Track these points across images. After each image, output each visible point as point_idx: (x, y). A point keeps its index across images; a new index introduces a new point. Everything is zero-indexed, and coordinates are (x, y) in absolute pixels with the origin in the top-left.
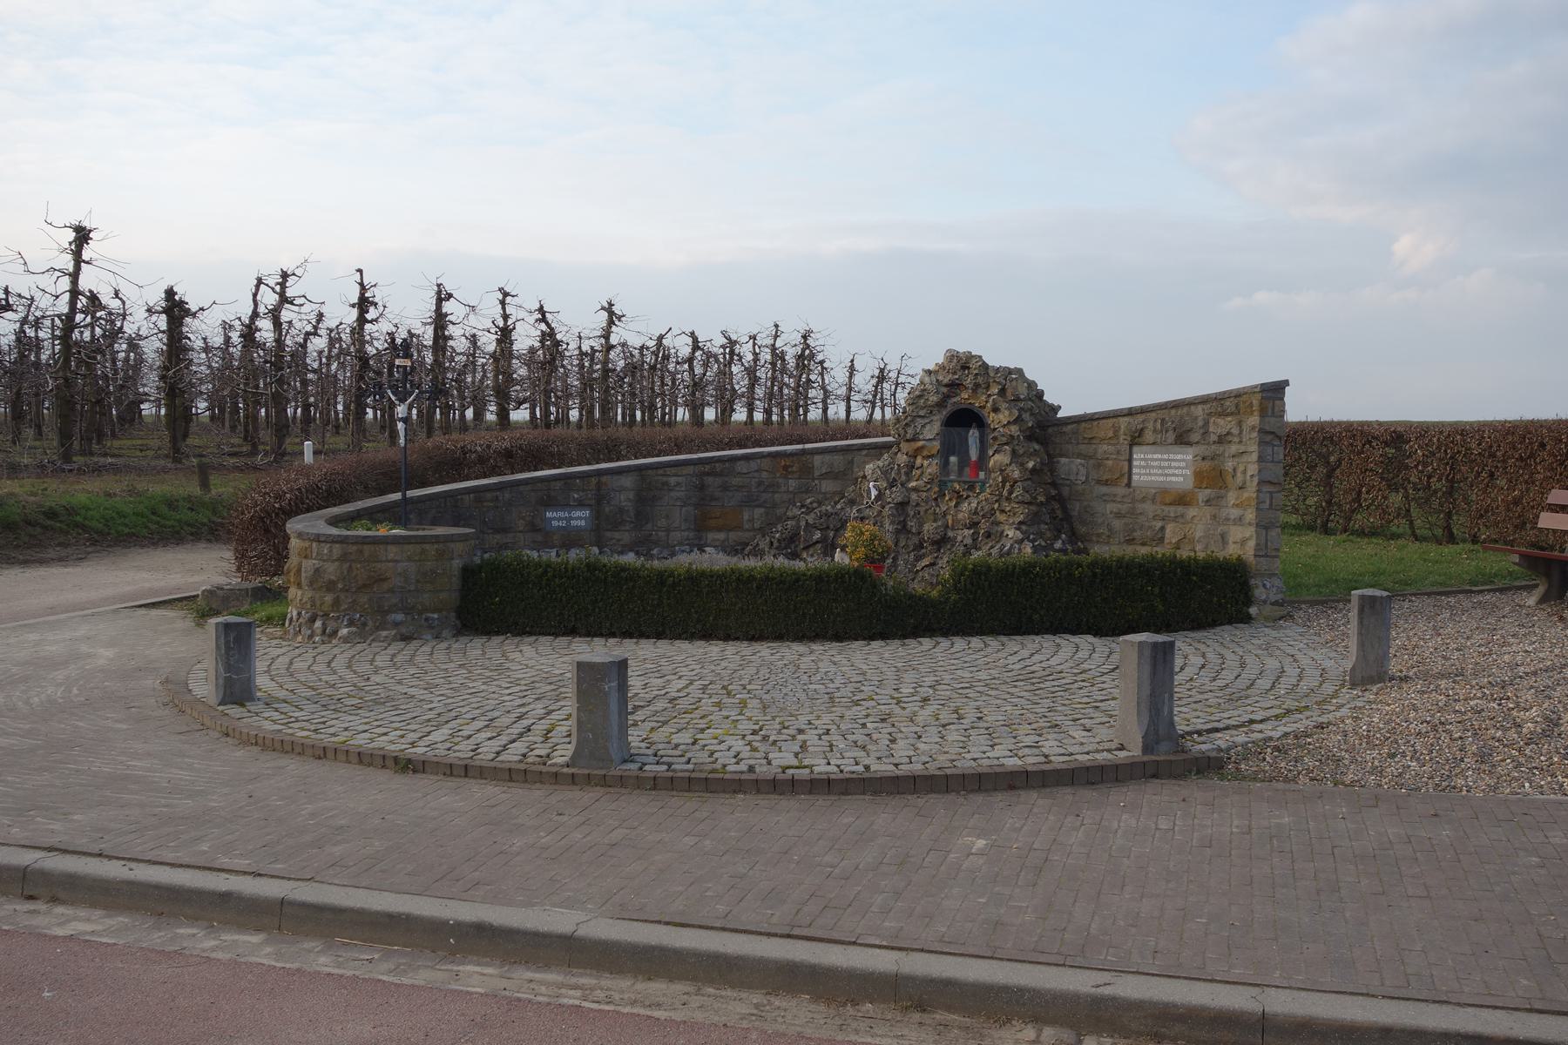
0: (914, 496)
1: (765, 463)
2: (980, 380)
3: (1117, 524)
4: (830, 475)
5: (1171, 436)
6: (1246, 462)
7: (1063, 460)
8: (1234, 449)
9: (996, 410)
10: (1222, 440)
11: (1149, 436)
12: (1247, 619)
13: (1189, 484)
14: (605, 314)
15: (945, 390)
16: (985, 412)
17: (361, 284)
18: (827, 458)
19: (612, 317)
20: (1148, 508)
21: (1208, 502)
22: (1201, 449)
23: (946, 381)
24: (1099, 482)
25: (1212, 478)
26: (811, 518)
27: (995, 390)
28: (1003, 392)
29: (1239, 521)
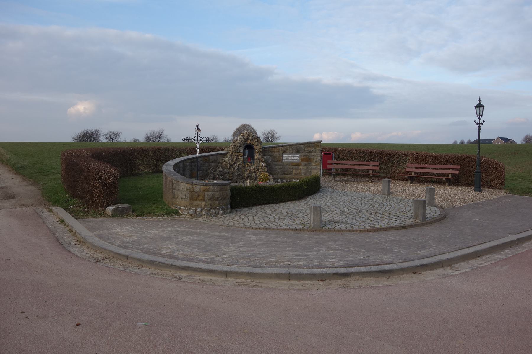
3: (279, 170)
4: (215, 162)
5: (294, 151)
6: (318, 158)
8: (313, 154)
9: (257, 145)
10: (310, 152)
11: (288, 151)
13: (299, 161)
18: (213, 157)
20: (288, 167)
22: (303, 154)
24: (275, 161)
25: (307, 160)
29: (315, 169)
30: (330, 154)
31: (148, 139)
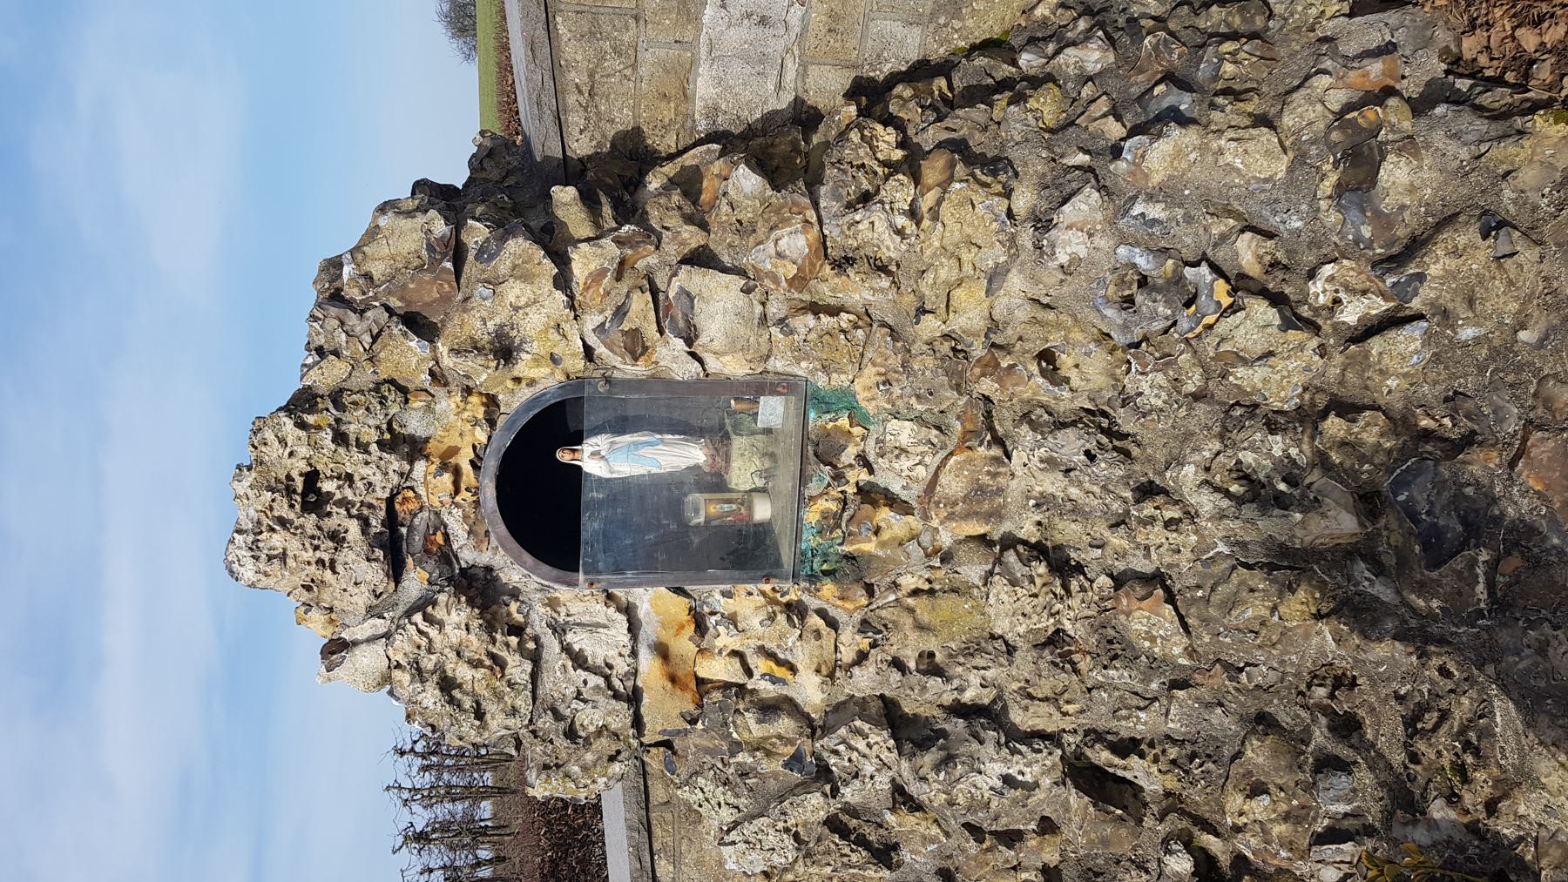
0: (864, 682)
2: (362, 425)
7: (704, 88)
9: (504, 351)
15: (416, 581)
16: (514, 401)
23: (374, 574)
27: (408, 356)
28: (419, 324)
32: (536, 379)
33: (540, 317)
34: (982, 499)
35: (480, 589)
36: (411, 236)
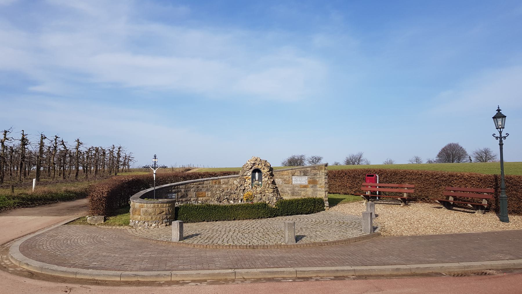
0: (246, 188)
1: (211, 181)
5: (302, 174)
6: (322, 180)
8: (318, 176)
10: (315, 175)
11: (296, 174)
12: (324, 210)
14: (77, 143)
17: (23, 134)
19: (79, 143)
21: (312, 187)
25: (313, 182)
26: (223, 193)
29: (320, 191)
30: (373, 176)
31: (348, 163)
32: (262, 171)
33: (265, 171)
34: (257, 193)
35: (251, 168)
36: (269, 165)
